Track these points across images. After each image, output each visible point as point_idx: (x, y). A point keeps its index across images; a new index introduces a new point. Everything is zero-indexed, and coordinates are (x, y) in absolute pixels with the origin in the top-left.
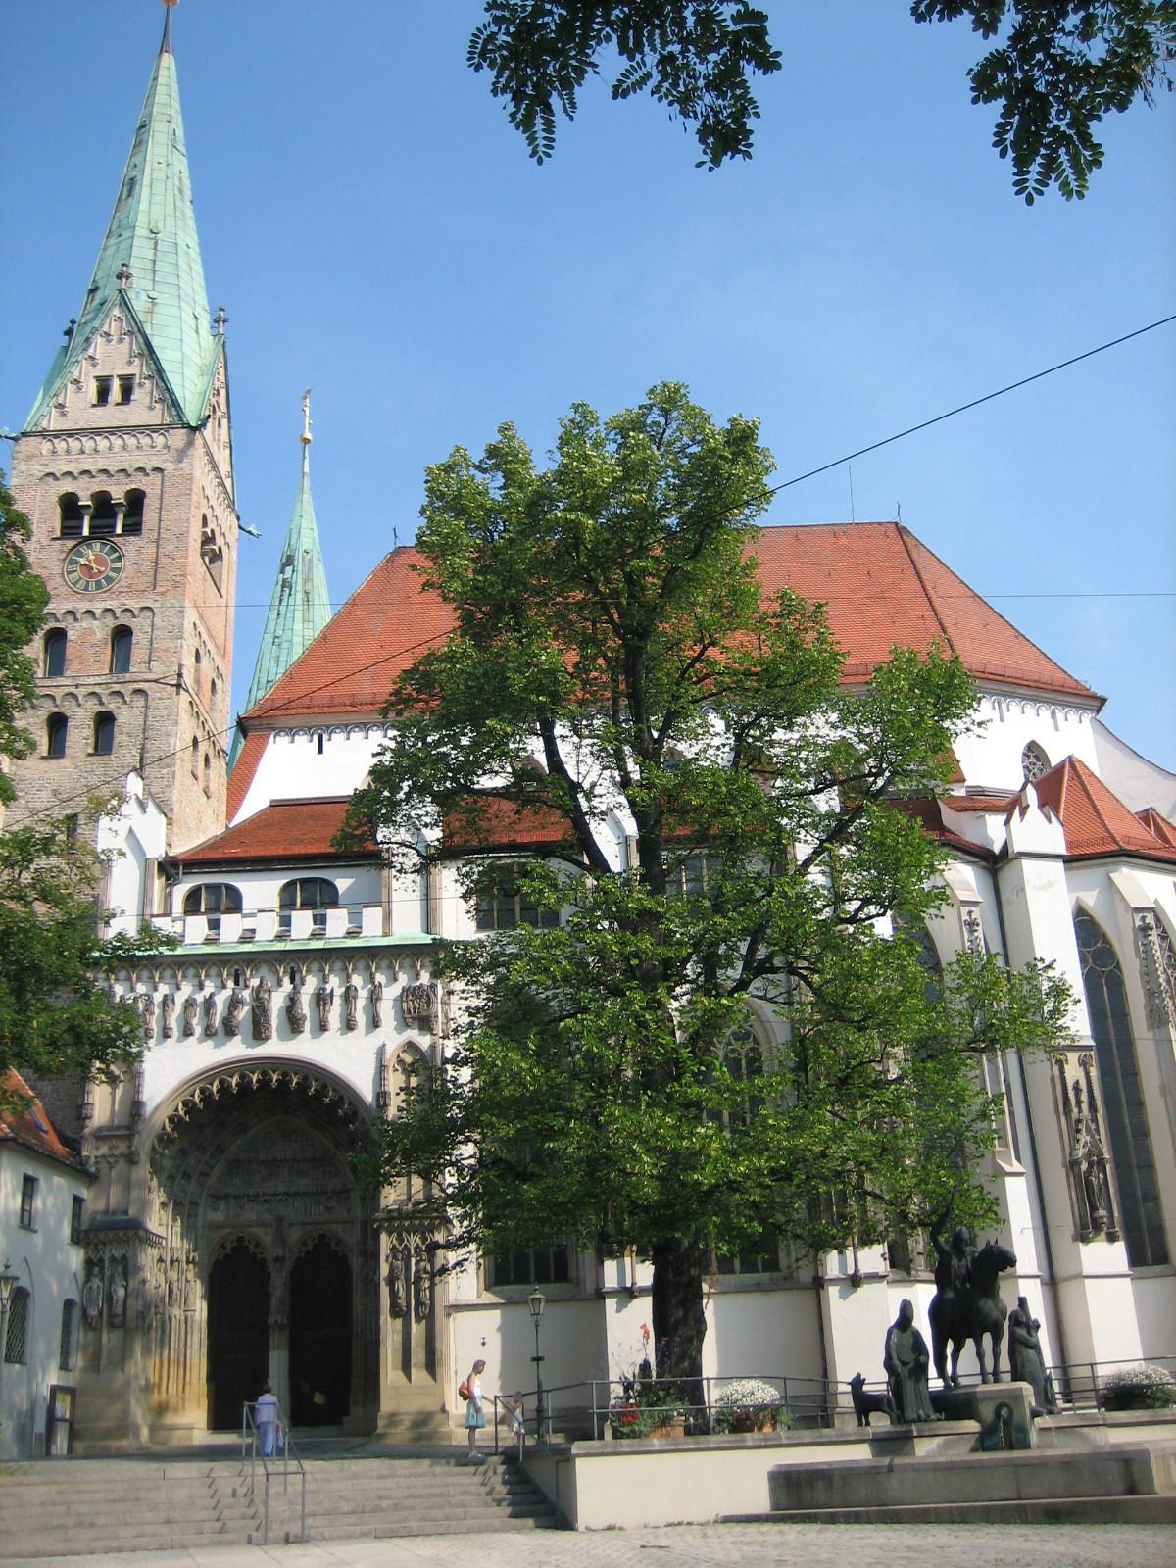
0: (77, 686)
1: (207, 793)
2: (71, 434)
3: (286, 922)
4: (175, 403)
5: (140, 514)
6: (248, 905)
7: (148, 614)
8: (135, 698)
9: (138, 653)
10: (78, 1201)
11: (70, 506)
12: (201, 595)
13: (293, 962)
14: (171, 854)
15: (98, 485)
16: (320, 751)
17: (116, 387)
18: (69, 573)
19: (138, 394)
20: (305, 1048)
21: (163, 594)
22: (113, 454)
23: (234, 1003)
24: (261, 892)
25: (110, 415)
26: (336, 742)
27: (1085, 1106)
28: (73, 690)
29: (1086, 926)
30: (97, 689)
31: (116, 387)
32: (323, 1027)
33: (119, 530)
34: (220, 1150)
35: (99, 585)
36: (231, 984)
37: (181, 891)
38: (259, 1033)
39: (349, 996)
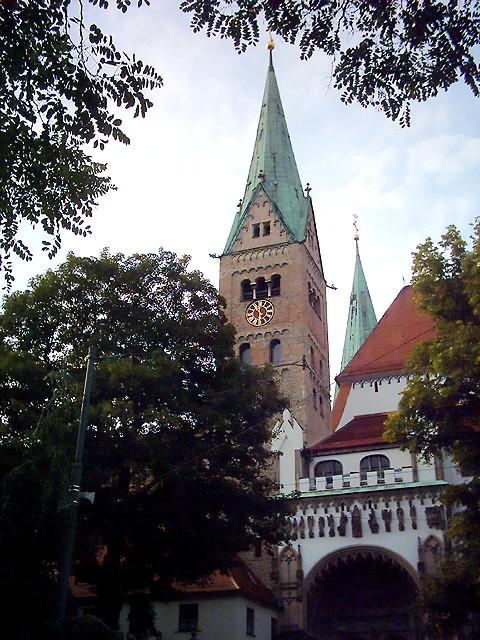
1: (322, 414)
3: (364, 477)
4: (289, 232)
10: (274, 621)
11: (246, 285)
13: (370, 497)
14: (307, 447)
16: (377, 391)
17: (261, 227)
22: (262, 259)
23: (344, 519)
24: (351, 462)
25: (262, 241)
26: (384, 385)
31: (261, 227)
32: (388, 529)
38: (358, 533)
39: (400, 512)
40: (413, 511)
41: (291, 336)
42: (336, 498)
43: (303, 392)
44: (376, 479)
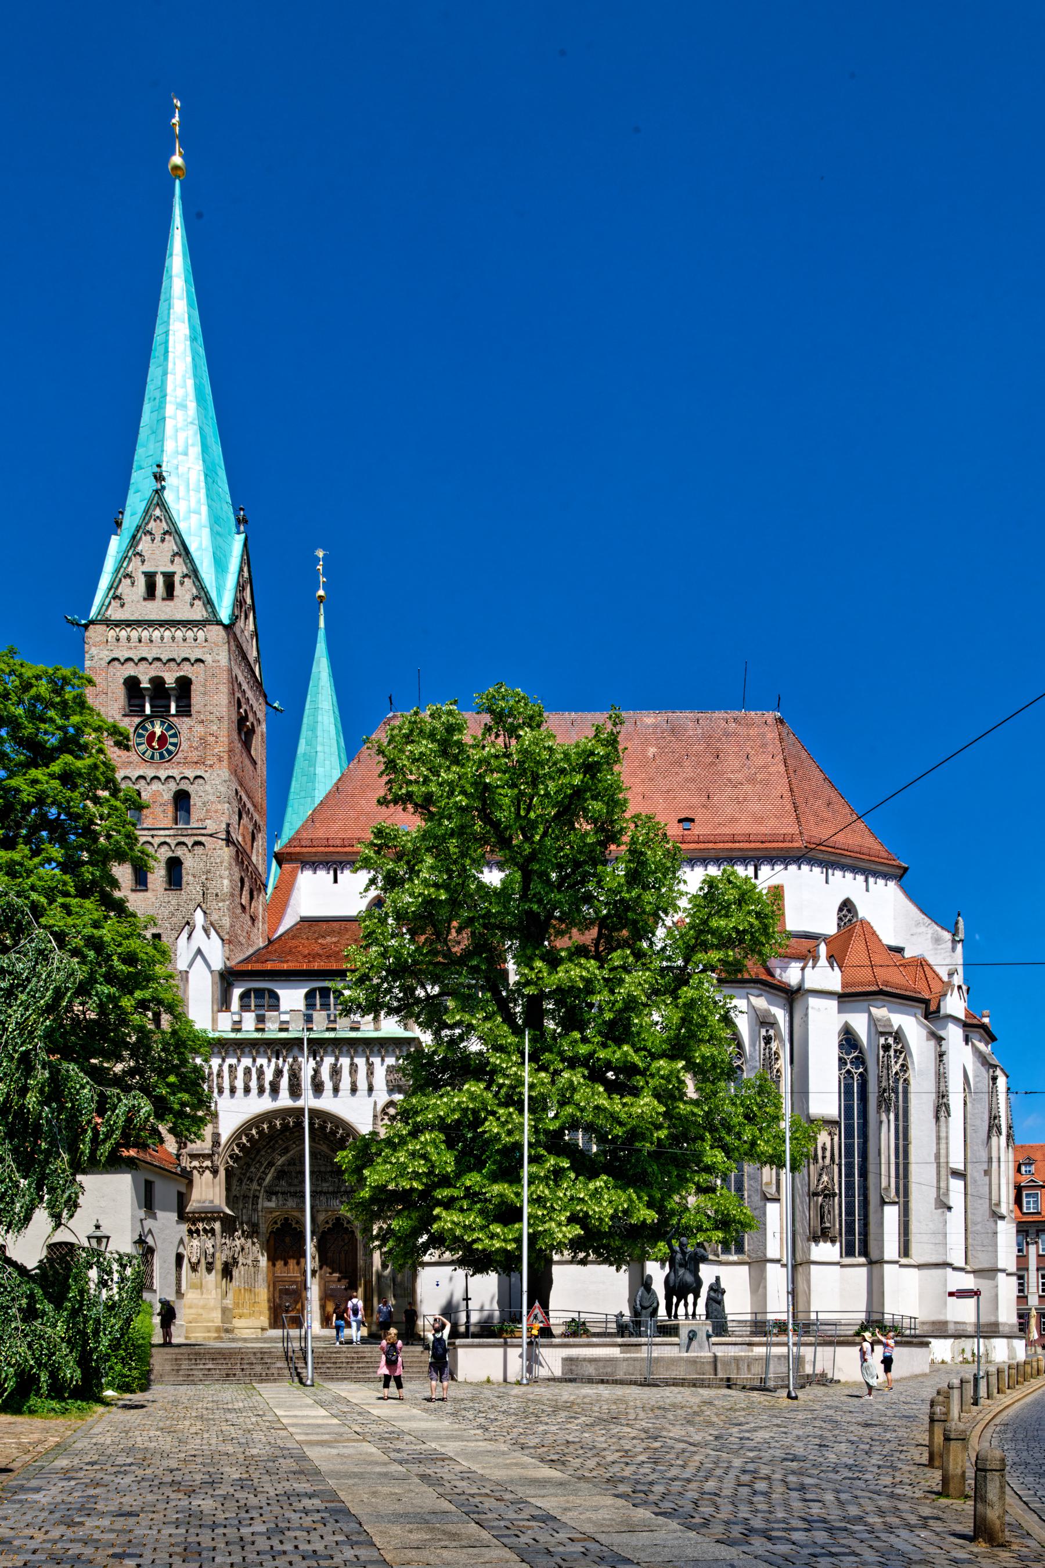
0: (153, 836)
2: (129, 624)
3: (309, 1019)
4: (209, 602)
5: (189, 697)
6: (284, 1006)
7: (201, 781)
8: (196, 848)
9: (196, 813)
11: (132, 684)
12: (240, 765)
13: (318, 1046)
14: (228, 964)
15: (154, 671)
17: (160, 581)
18: (139, 744)
19: (178, 590)
20: (327, 1103)
21: (211, 766)
23: (278, 1073)
27: (828, 1161)
28: (150, 839)
29: (848, 1040)
30: (168, 840)
31: (160, 581)
32: (336, 1090)
33: (173, 711)
34: (271, 1164)
35: (162, 756)
36: (274, 1060)
37: (237, 992)
38: (295, 1091)
39: (354, 1069)
40: (370, 1073)
41: (208, 787)
42: (269, 1043)
43: (226, 882)
44: (325, 1024)
